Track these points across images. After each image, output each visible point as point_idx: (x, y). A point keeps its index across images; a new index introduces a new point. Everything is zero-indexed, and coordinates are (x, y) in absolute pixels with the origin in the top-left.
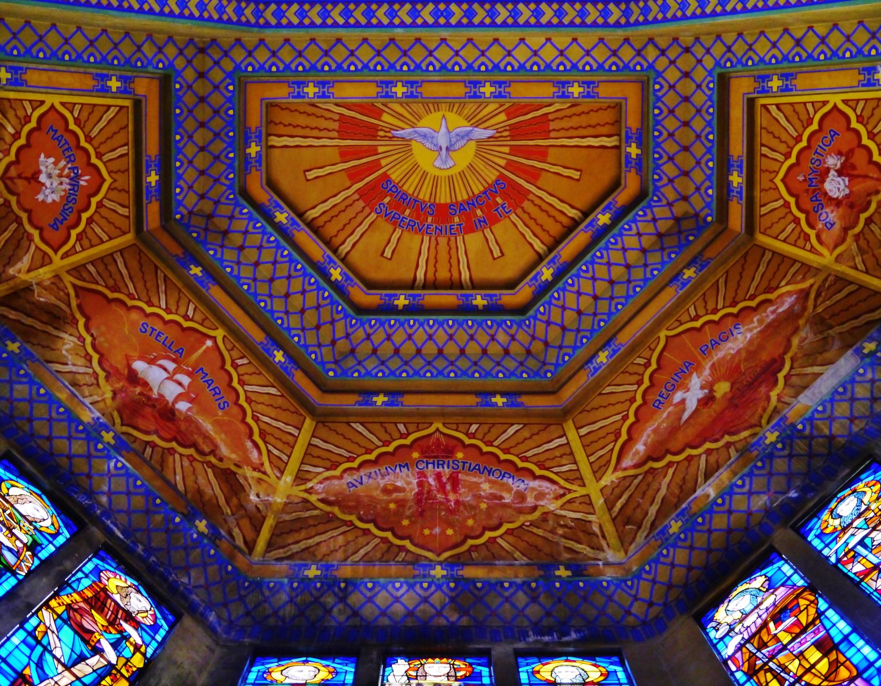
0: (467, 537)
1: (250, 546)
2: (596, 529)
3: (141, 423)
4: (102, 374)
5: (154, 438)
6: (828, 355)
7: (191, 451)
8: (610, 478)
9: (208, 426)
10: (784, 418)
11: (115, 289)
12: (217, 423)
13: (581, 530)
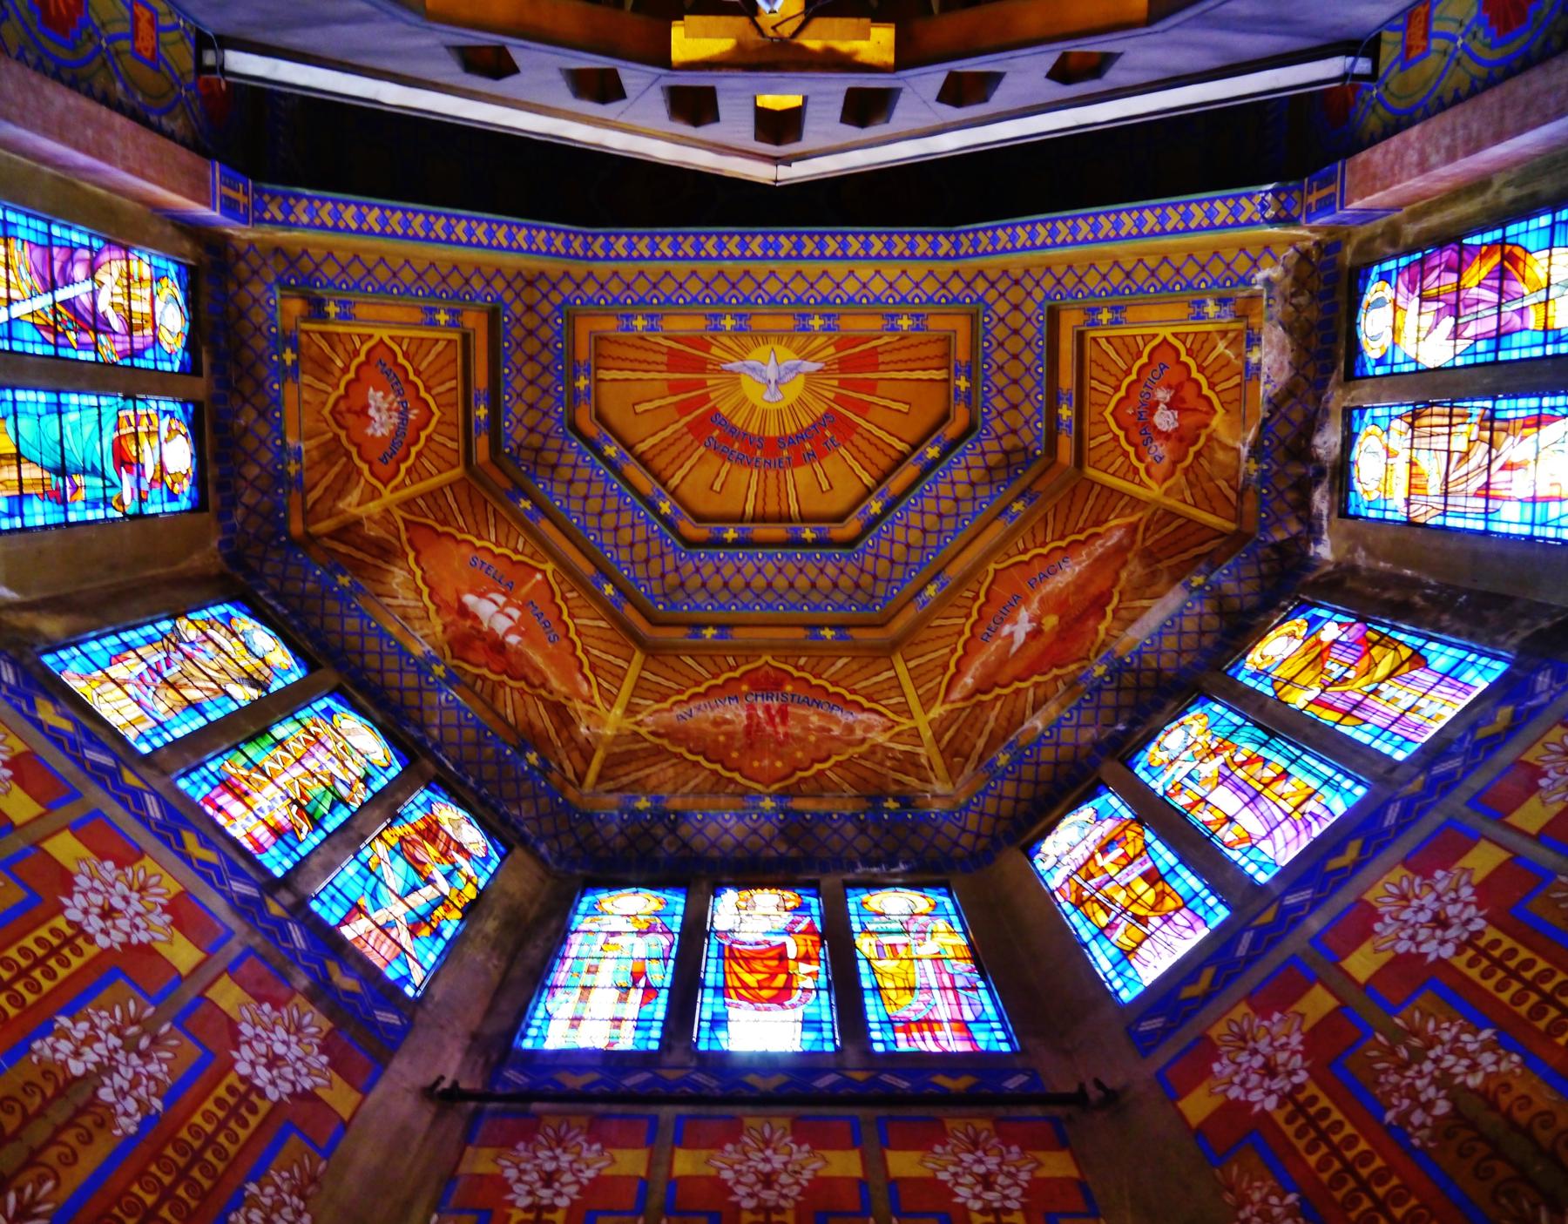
0: (795, 769)
1: (581, 778)
2: (924, 761)
3: (471, 656)
4: (432, 608)
5: (485, 671)
6: (1157, 589)
7: (522, 684)
8: (937, 711)
9: (538, 660)
10: (1111, 652)
11: (444, 523)
12: (550, 657)
13: (909, 763)
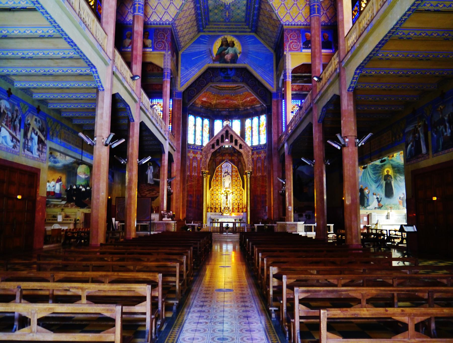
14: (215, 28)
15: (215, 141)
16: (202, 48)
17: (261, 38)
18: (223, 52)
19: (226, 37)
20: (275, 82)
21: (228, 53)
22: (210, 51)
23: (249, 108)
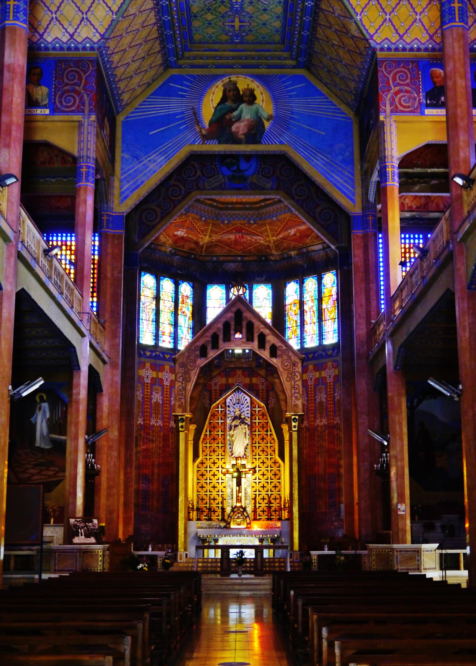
1: (201, 252)
8: (274, 238)
9: (190, 236)
14: (208, 58)
15: (207, 338)
16: (175, 106)
17: (321, 81)
18: (227, 117)
19: (233, 78)
20: (358, 190)
21: (239, 118)
22: (195, 113)
23: (293, 253)
